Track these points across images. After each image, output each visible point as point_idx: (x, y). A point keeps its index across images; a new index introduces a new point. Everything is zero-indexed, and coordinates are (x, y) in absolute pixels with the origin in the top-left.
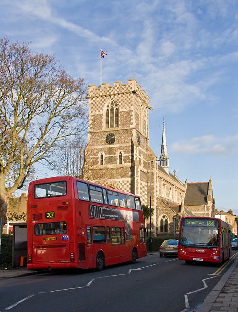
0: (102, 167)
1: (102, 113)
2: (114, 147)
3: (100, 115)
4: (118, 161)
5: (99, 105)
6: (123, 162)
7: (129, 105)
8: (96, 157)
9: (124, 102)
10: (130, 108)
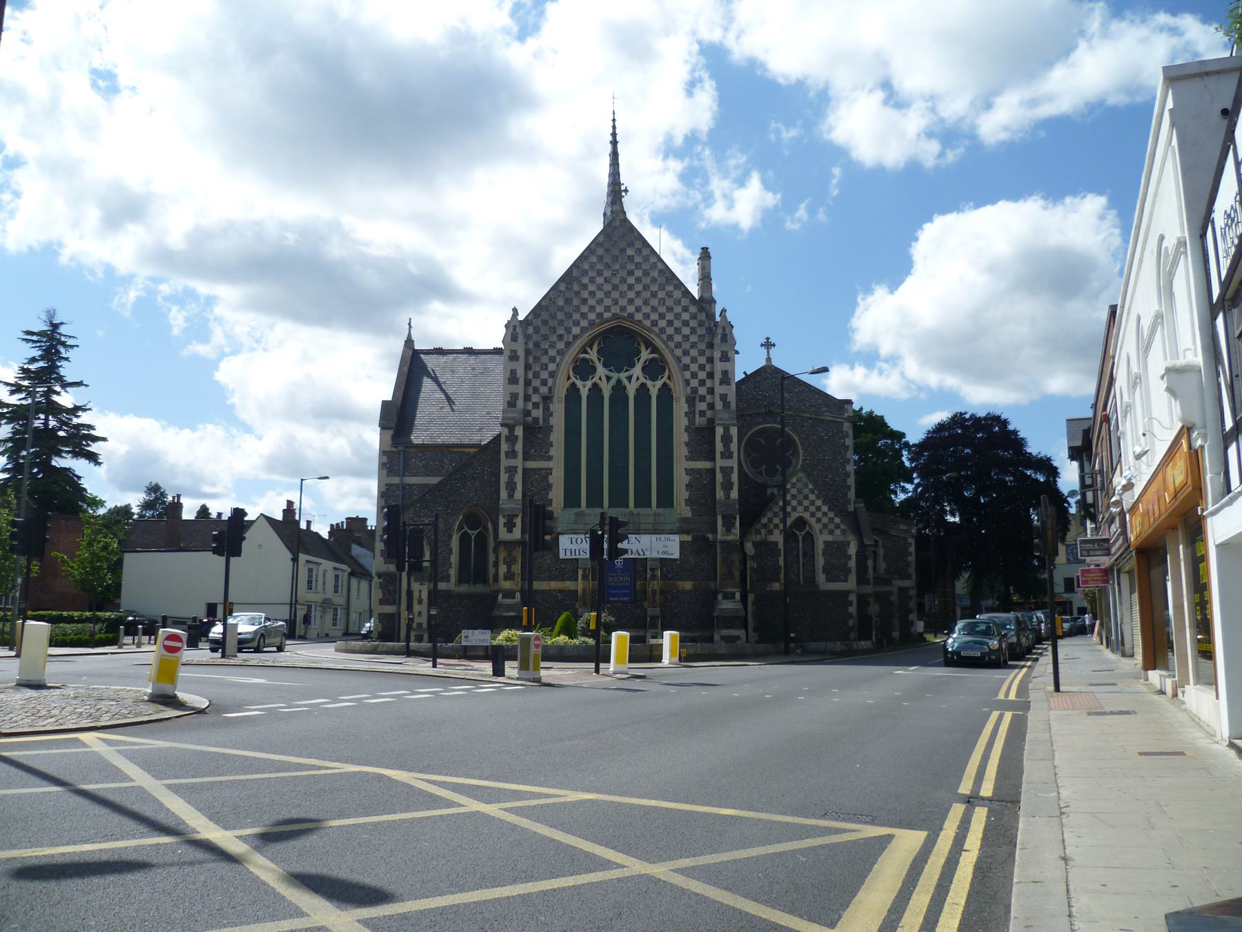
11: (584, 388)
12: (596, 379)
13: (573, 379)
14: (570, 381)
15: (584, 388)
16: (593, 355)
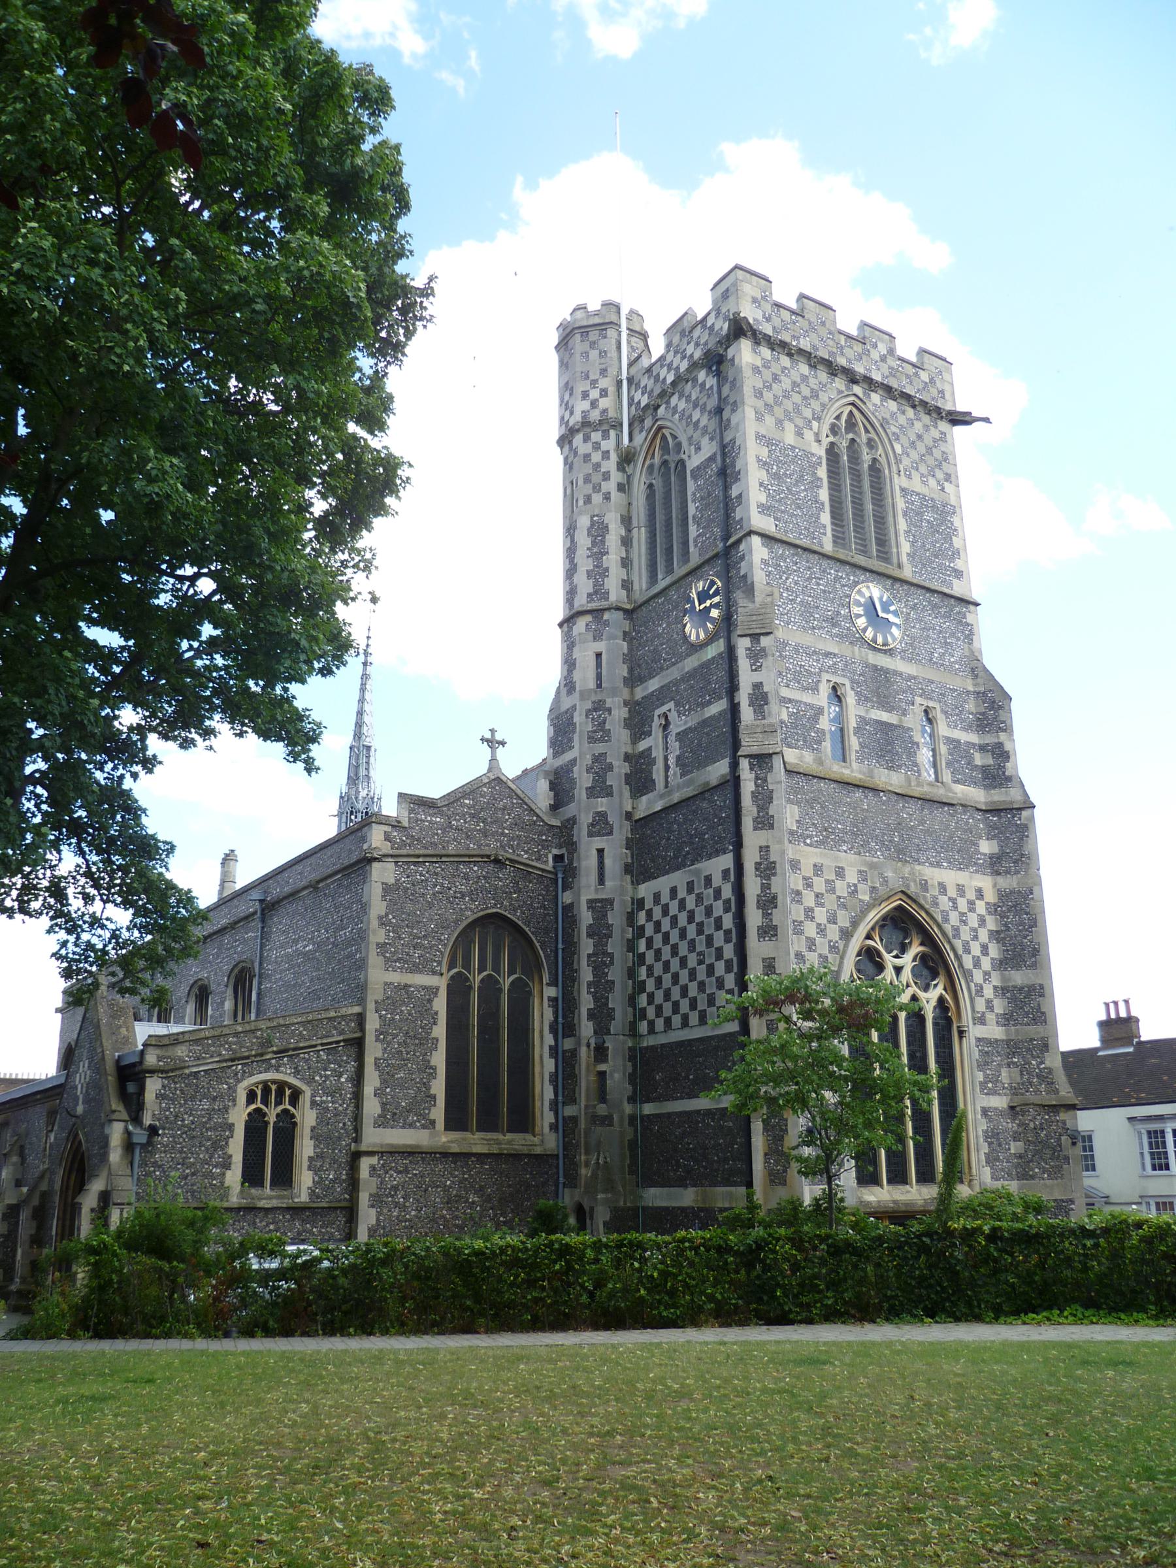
0: (838, 770)
2: (895, 673)
5: (797, 398)
6: (947, 776)
8: (807, 698)
9: (913, 444)
10: (943, 490)
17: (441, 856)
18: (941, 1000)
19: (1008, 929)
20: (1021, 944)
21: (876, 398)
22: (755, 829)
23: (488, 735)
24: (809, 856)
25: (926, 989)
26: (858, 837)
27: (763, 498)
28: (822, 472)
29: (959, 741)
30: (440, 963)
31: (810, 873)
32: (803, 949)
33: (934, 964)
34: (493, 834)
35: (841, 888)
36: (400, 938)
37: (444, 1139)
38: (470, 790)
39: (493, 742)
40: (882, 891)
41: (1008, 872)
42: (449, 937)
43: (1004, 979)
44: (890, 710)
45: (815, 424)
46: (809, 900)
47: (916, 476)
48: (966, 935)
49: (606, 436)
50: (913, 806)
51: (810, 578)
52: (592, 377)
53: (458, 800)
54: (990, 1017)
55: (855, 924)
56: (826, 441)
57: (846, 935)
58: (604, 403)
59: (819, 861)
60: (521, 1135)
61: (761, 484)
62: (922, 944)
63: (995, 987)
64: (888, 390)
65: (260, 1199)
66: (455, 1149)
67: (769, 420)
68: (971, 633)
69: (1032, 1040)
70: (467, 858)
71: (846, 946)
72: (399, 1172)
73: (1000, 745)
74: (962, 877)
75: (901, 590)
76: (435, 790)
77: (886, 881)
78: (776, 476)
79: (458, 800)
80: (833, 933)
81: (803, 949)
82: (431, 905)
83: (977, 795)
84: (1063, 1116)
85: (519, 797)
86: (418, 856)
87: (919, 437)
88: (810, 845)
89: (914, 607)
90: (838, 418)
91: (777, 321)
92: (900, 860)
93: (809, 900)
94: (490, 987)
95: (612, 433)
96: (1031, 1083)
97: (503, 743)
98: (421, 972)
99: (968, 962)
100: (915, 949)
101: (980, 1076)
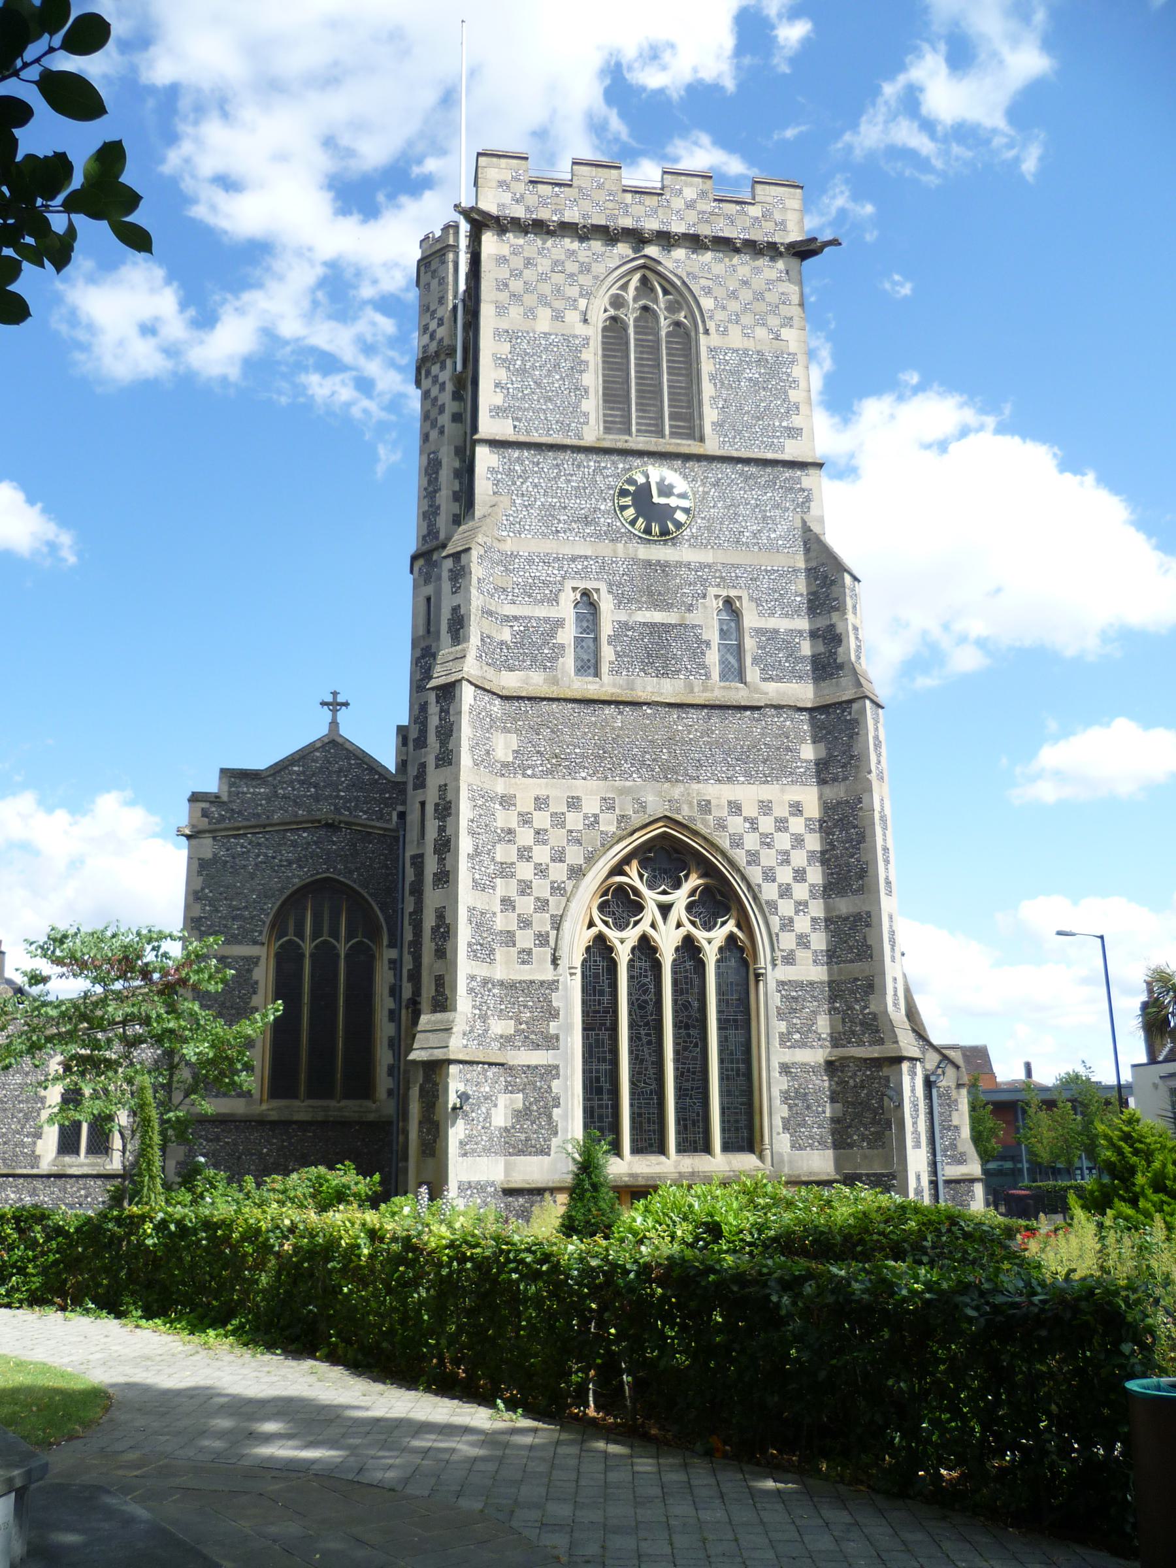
0: (589, 687)
1: (580, 330)
2: (679, 564)
3: (566, 338)
4: (713, 658)
5: (558, 278)
6: (753, 673)
7: (773, 321)
8: (541, 612)
9: (733, 295)
10: (777, 338)
11: (624, 943)
12: (644, 926)
13: (601, 927)
14: (594, 930)
15: (624, 943)
16: (633, 876)
17: (265, 826)
18: (731, 938)
19: (834, 848)
20: (848, 864)
21: (680, 253)
22: (437, 767)
23: (330, 699)
24: (526, 790)
25: (709, 926)
26: (603, 761)
27: (498, 400)
28: (593, 355)
29: (776, 631)
30: (261, 932)
31: (529, 806)
32: (513, 893)
33: (718, 900)
34: (326, 799)
35: (574, 820)
36: (217, 911)
37: (264, 1107)
38: (302, 756)
39: (335, 705)
40: (637, 820)
41: (835, 780)
42: (272, 906)
43: (828, 908)
44: (666, 606)
45: (582, 303)
46: (525, 837)
47: (735, 331)
48: (768, 858)
49: (443, 368)
50: (693, 714)
51: (558, 476)
52: (432, 309)
53: (286, 768)
54: (803, 955)
55: (591, 859)
56: (599, 318)
57: (577, 873)
58: (441, 332)
59: (543, 792)
60: (358, 1102)
61: (497, 385)
62: (700, 877)
63: (814, 920)
64: (695, 242)
65: (70, 1166)
66: (274, 1116)
67: (515, 312)
68: (808, 499)
69: (857, 979)
70: (294, 825)
71: (576, 887)
72: (211, 1141)
73: (833, 626)
74: (768, 792)
75: (697, 468)
76: (260, 761)
77: (643, 807)
78: (522, 371)
79: (286, 768)
80: (558, 872)
81: (513, 893)
82: (252, 876)
83: (804, 692)
84: (886, 1071)
85: (357, 758)
86: (239, 829)
87: (745, 283)
88: (533, 776)
89: (716, 484)
90: (624, 287)
91: (531, 200)
92: (667, 780)
93: (525, 837)
94: (325, 956)
95: (449, 362)
96: (853, 1033)
97: (346, 704)
98: (240, 943)
99: (769, 892)
100: (694, 881)
101: (782, 1027)
